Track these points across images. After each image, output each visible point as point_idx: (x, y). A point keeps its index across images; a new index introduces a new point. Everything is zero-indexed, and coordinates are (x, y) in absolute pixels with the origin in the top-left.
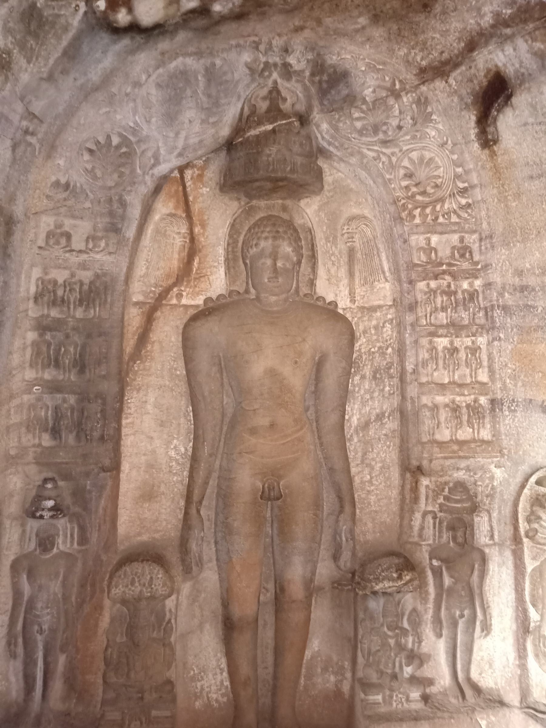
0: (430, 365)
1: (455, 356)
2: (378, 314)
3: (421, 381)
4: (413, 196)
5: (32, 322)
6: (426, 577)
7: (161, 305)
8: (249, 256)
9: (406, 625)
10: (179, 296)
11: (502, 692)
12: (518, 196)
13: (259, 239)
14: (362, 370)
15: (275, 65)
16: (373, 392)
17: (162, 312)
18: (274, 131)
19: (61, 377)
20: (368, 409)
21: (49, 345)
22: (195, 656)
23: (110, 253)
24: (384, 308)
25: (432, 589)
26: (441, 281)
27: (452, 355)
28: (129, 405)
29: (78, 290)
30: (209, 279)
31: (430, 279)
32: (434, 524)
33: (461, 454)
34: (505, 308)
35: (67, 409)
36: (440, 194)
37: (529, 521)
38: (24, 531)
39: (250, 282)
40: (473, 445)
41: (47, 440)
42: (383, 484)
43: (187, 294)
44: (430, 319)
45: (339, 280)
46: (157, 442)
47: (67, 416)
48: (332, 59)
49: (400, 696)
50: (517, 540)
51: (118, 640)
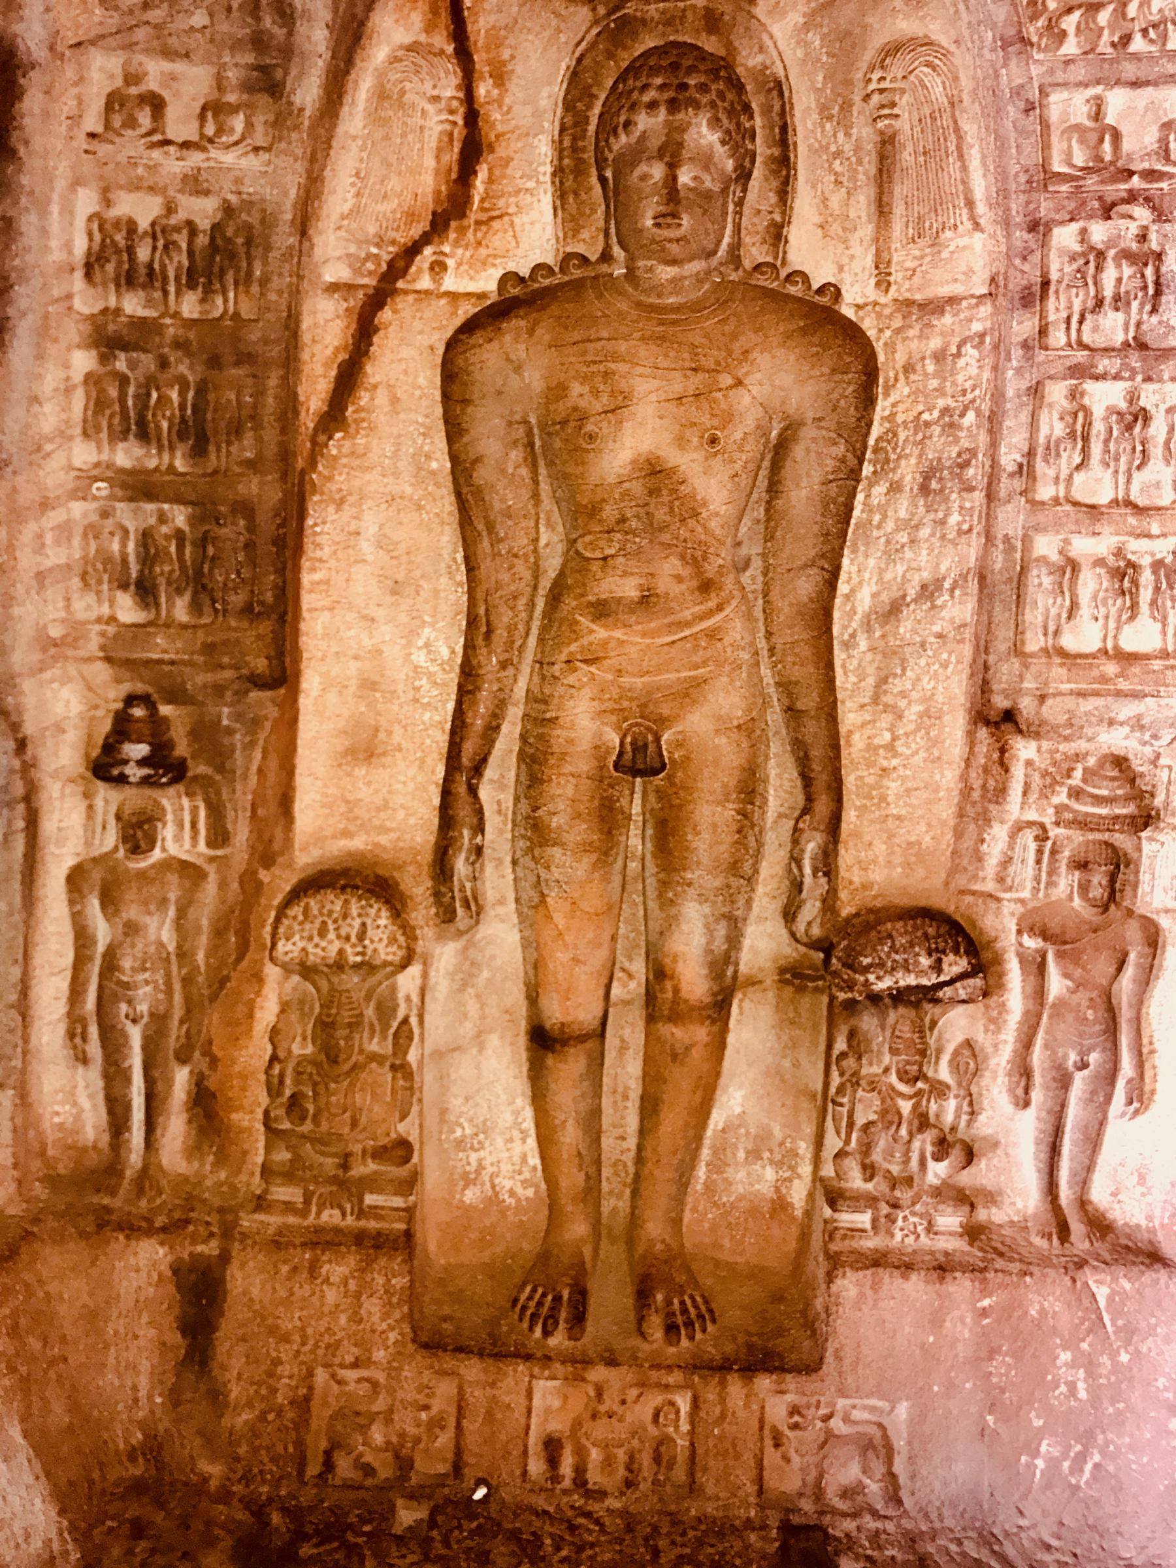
0: (1064, 455)
1: (1137, 429)
2: (948, 319)
3: (1038, 498)
5: (81, 327)
6: (1001, 975)
7: (395, 292)
8: (611, 157)
9: (943, 1072)
10: (438, 268)
11: (1160, 1236)
13: (633, 107)
14: (894, 470)
16: (917, 527)
17: (395, 312)
19: (152, 463)
20: (900, 569)
21: (124, 381)
22: (467, 1099)
23: (256, 149)
24: (964, 303)
26: (1123, 223)
27: (1129, 428)
28: (318, 539)
29: (184, 246)
30: (512, 224)
31: (1090, 217)
32: (1040, 852)
33: (1123, 685)
35: (167, 537)
38: (90, 807)
39: (613, 230)
40: (1157, 665)
41: (128, 610)
42: (922, 754)
43: (459, 264)
44: (1079, 330)
45: (850, 228)
46: (385, 631)
47: (168, 553)
49: (912, 1219)
51: (297, 1049)
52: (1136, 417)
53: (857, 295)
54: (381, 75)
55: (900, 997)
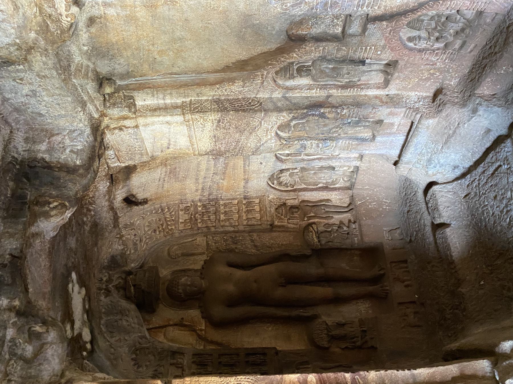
4: (163, 229)
12: (168, 191)
15: (107, 286)
18: (134, 286)
25: (316, 220)
33: (265, 210)
34: (209, 195)
36: (163, 219)
37: (287, 187)
48: (106, 262)
50: (295, 191)
52: (225, 213)
53: (204, 257)
54: (169, 340)
55: (318, 237)
